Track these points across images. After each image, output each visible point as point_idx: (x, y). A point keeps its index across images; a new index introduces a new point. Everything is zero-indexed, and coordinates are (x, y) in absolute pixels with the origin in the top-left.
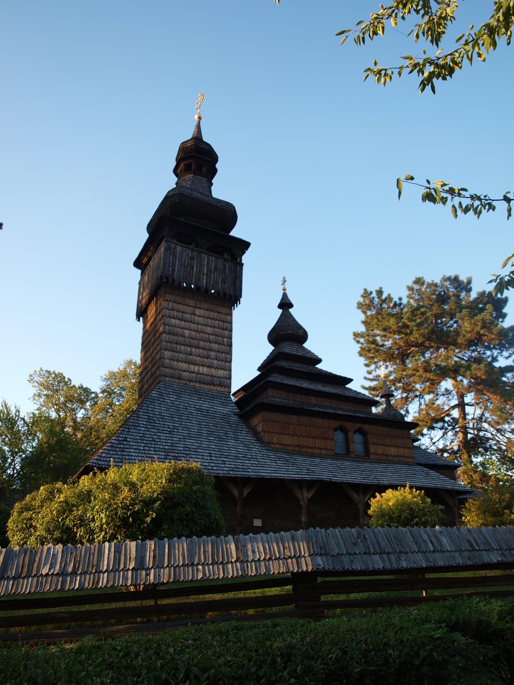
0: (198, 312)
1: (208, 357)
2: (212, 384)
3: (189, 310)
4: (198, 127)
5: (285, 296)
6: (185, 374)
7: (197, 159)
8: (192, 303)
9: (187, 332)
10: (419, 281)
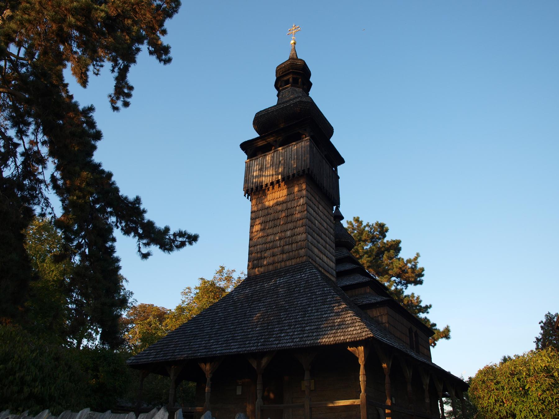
0: (320, 207)
1: (326, 248)
2: (328, 272)
3: (317, 203)
6: (318, 259)
7: (294, 76)
9: (316, 222)
10: (357, 220)
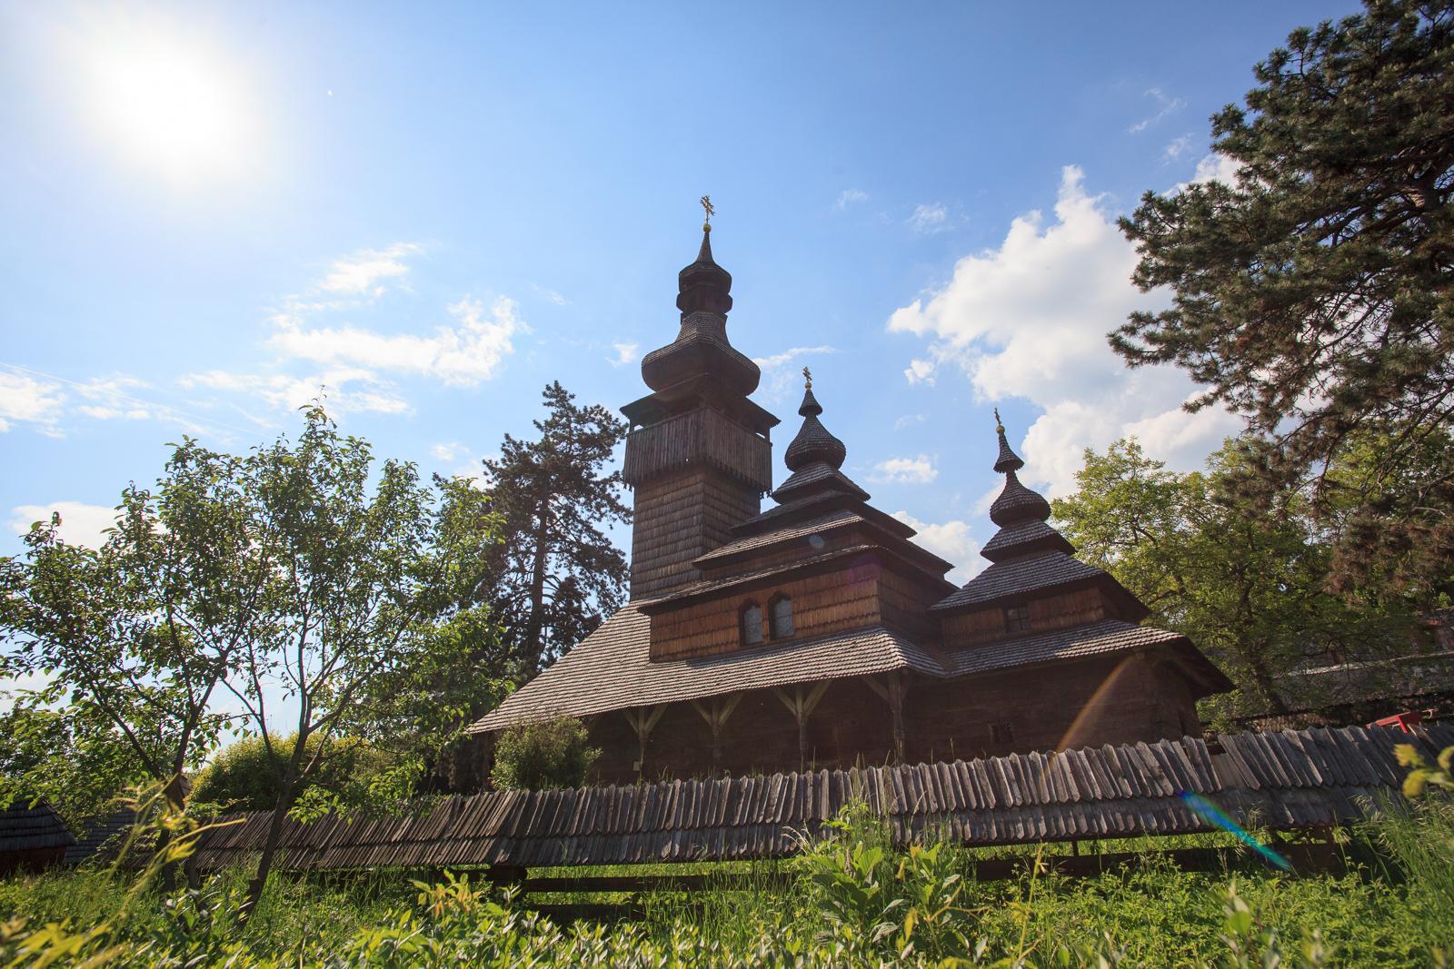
1: (675, 551)
4: (706, 248)
5: (809, 395)
7: (704, 289)
8: (660, 491)
